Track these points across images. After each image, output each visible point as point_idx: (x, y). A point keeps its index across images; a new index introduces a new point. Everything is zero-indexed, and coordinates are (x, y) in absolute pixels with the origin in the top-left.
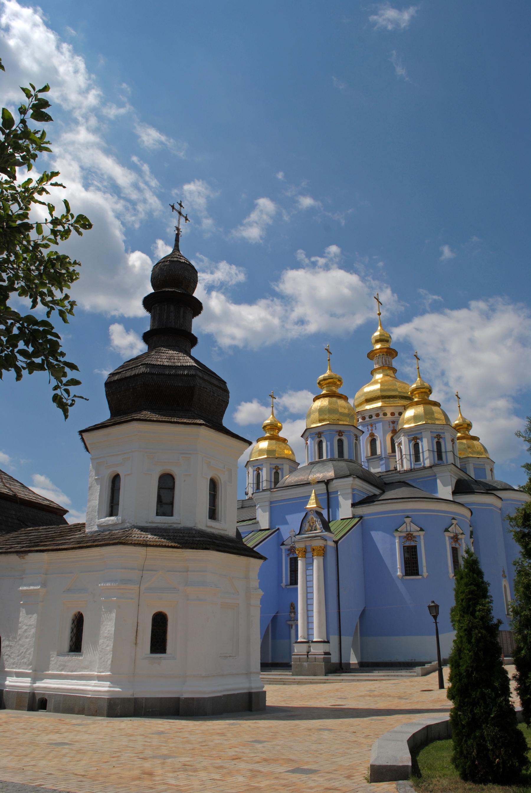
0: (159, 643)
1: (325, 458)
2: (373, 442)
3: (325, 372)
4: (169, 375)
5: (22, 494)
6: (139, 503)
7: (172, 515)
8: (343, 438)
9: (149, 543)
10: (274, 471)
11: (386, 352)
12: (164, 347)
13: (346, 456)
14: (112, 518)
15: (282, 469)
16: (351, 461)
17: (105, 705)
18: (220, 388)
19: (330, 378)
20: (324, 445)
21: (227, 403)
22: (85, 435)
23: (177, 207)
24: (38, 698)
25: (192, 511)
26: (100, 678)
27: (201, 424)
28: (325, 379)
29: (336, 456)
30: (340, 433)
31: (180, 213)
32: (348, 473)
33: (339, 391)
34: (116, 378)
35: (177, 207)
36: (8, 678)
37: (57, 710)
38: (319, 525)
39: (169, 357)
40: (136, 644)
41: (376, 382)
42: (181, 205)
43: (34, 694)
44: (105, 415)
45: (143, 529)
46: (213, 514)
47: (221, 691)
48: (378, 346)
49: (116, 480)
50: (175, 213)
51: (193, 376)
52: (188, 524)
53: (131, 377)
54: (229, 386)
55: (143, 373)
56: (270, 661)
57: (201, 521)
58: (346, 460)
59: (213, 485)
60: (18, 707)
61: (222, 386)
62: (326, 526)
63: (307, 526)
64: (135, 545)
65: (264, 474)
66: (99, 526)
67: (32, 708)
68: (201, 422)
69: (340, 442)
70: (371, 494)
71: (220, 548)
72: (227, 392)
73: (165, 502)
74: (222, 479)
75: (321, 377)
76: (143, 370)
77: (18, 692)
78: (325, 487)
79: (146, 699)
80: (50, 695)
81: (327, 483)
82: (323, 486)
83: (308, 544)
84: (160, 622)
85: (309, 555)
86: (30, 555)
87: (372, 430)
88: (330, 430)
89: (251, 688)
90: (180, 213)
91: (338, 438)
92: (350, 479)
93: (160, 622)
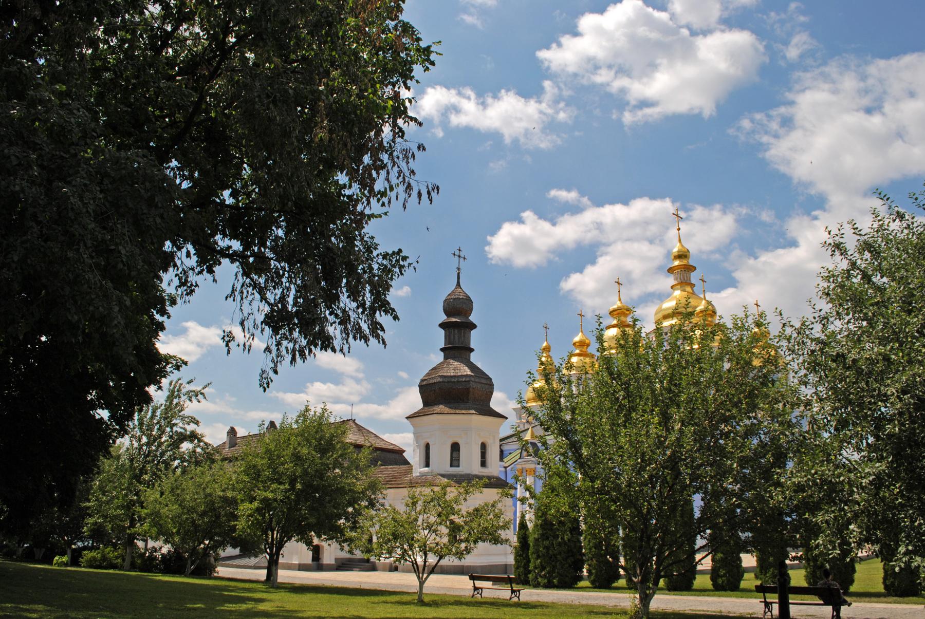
6: (441, 459)
12: (453, 359)
23: (457, 253)
25: (470, 463)
35: (457, 253)
45: (443, 476)
46: (483, 464)
49: (427, 446)
50: (456, 257)
51: (468, 381)
52: (468, 472)
55: (439, 382)
57: (477, 469)
60: (384, 570)
67: (390, 570)
68: (474, 412)
73: (455, 460)
76: (439, 380)
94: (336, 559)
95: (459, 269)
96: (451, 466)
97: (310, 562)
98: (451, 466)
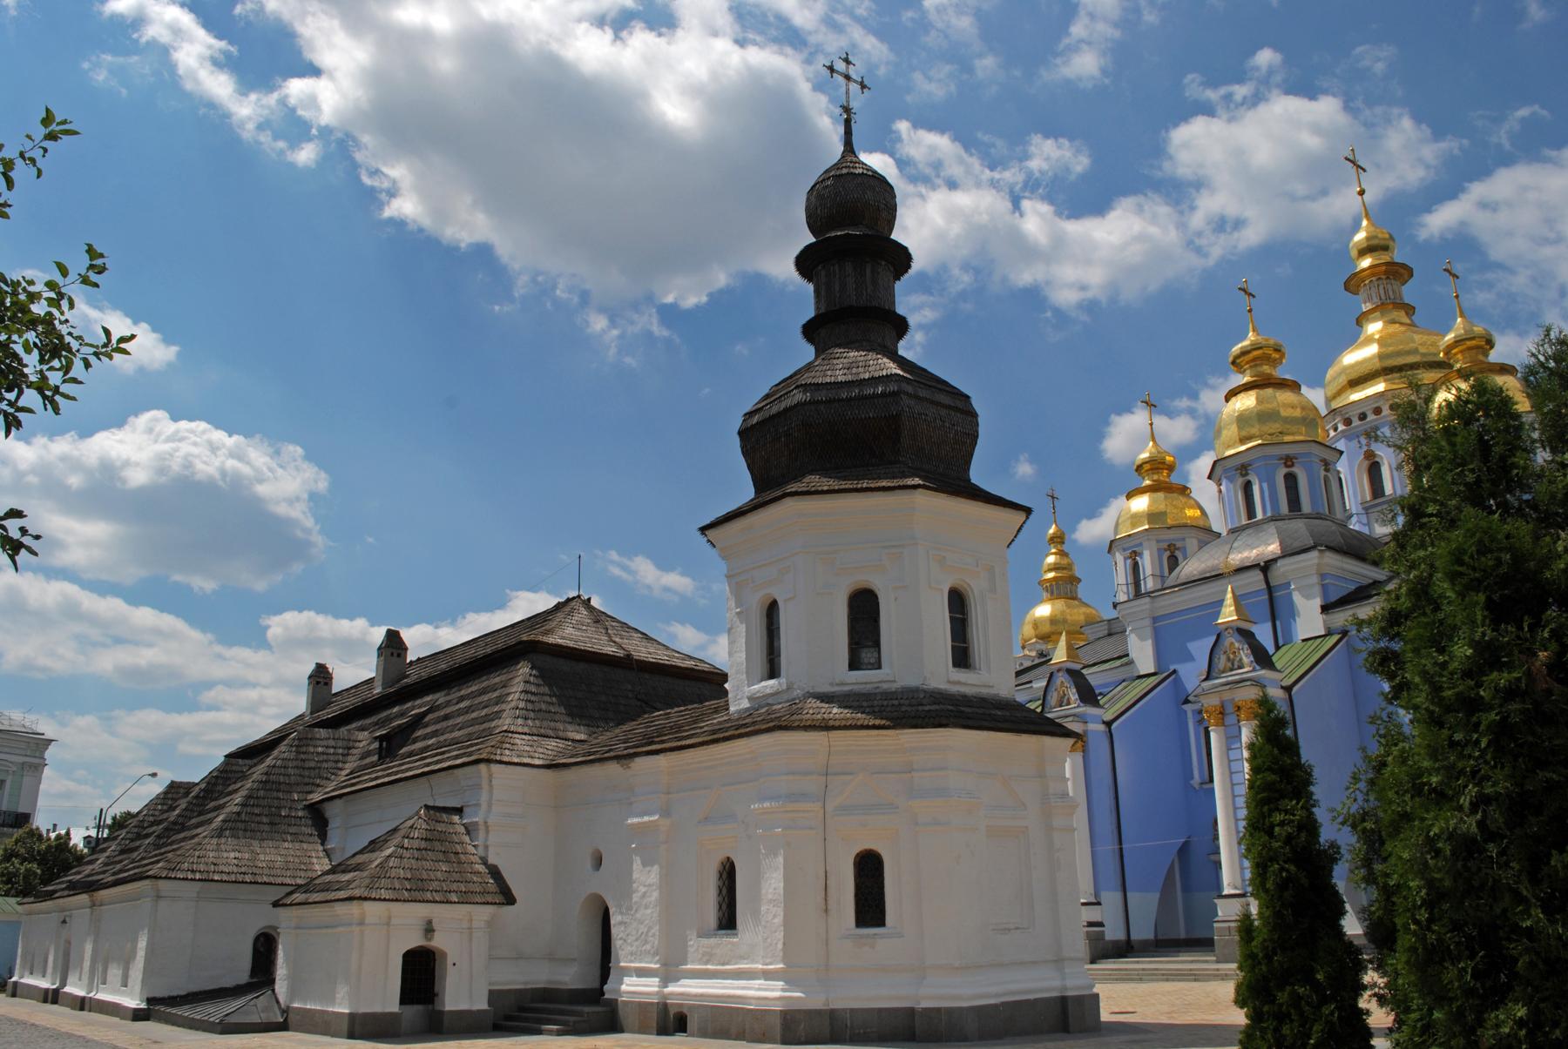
0: (870, 909)
1: (1260, 515)
2: (1374, 470)
3: (1244, 338)
4: (850, 400)
5: (643, 652)
6: (818, 649)
7: (879, 667)
8: (1296, 470)
9: (831, 723)
10: (1168, 553)
11: (1386, 272)
12: (839, 346)
13: (1306, 507)
14: (772, 682)
15: (1184, 550)
16: (1319, 517)
17: (777, 1023)
18: (956, 409)
19: (1256, 347)
20: (1256, 489)
21: (974, 437)
22: (711, 533)
23: (840, 66)
24: (672, 1011)
25: (916, 653)
26: (767, 975)
27: (918, 486)
28: (1244, 353)
29: (1284, 508)
30: (1289, 461)
31: (848, 77)
32: (1312, 543)
33: (1282, 372)
34: (755, 419)
35: (840, 66)
36: (626, 979)
37: (704, 1033)
38: (1246, 657)
39: (859, 364)
40: (826, 911)
41: (1369, 340)
42: (847, 61)
43: (665, 1005)
44: (746, 491)
45: (826, 698)
46: (962, 658)
47: (997, 995)
48: (1366, 263)
50: (841, 79)
51: (894, 394)
52: (911, 681)
53: (779, 414)
54: (977, 404)
55: (799, 405)
56: (1183, 935)
57: (940, 674)
58: (1308, 517)
59: (958, 602)
60: (643, 1030)
61: (959, 404)
62: (1263, 658)
63: (1221, 662)
64: (807, 728)
65: (1147, 563)
66: (750, 699)
67: (663, 1030)
68: (917, 481)
69: (1291, 480)
70: (1366, 582)
71: (970, 723)
72: (974, 415)
74: (976, 589)
75: (1236, 349)
76: (798, 397)
77: (640, 1004)
78: (1261, 576)
79: (852, 1010)
80: (692, 1007)
81: (1265, 567)
82: (1257, 576)
83: (1227, 696)
84: (869, 868)
85: (1231, 719)
86: (638, 760)
87: (1368, 445)
88: (1265, 457)
89: (1066, 989)
90: (848, 77)
91: (1284, 471)
92: (1314, 554)
93: (869, 868)
94: (494, 996)
95: (847, 110)
96: (854, 665)
97: (393, 1006)
98: (854, 665)
